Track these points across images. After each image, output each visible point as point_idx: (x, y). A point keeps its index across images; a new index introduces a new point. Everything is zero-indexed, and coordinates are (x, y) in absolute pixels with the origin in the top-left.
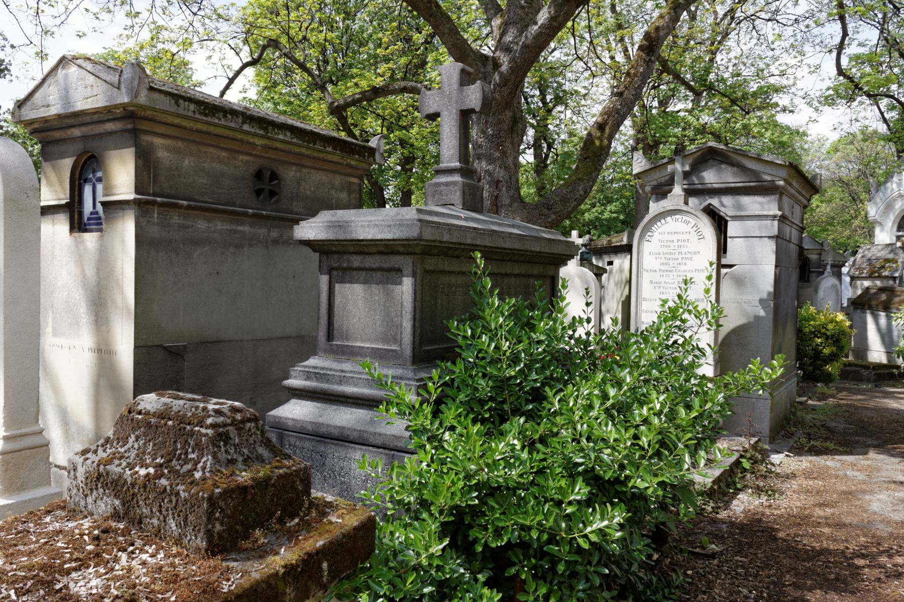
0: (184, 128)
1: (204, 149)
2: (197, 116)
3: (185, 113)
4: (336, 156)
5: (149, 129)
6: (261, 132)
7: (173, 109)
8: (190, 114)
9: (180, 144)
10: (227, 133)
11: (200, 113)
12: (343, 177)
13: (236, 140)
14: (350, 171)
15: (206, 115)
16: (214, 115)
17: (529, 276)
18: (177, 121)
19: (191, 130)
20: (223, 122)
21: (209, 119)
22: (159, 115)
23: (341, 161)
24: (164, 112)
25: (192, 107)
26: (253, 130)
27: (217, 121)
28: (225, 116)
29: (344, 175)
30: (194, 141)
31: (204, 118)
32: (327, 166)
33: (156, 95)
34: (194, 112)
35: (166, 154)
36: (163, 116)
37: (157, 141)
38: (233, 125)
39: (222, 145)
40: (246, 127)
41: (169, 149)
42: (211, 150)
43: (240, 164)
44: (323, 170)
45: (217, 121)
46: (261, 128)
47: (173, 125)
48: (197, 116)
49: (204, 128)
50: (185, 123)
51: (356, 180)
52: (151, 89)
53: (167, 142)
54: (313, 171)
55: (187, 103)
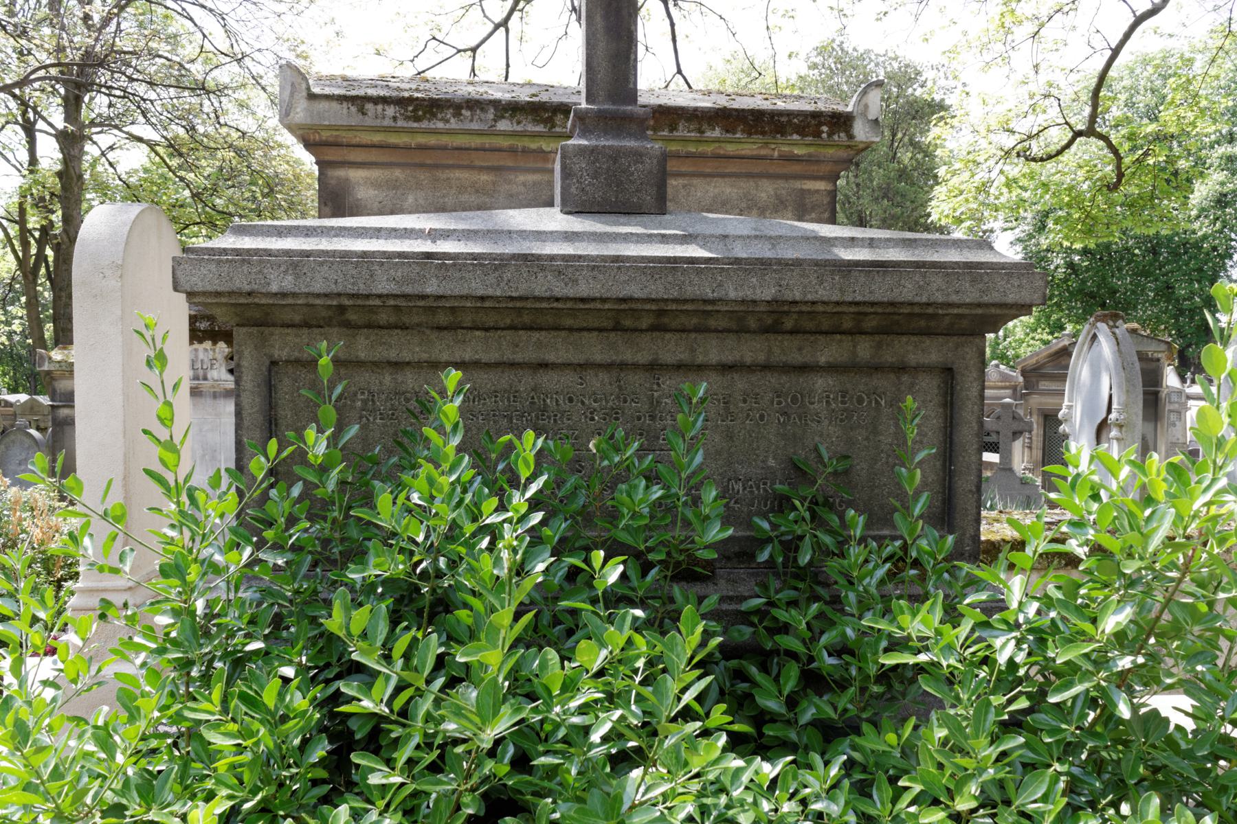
0: (395, 147)
1: (443, 175)
2: (401, 123)
3: (378, 122)
4: (749, 146)
5: (340, 159)
6: (540, 128)
7: (356, 119)
8: (387, 122)
9: (398, 173)
10: (476, 141)
11: (407, 118)
12: (781, 183)
13: (500, 150)
14: (796, 168)
15: (417, 119)
16: (434, 115)
17: (804, 369)
18: (377, 138)
19: (407, 148)
20: (454, 124)
21: (424, 124)
22: (344, 134)
23: (763, 152)
24: (350, 128)
25: (391, 111)
26: (519, 128)
27: (440, 125)
28: (457, 114)
29: (786, 177)
30: (422, 166)
31: (415, 125)
32: (732, 168)
33: (324, 105)
34: (395, 118)
35: (372, 192)
36: (350, 134)
37: (355, 175)
38: (475, 126)
39: (477, 163)
40: (504, 125)
41: (376, 185)
42: (458, 174)
43: (522, 189)
44: (723, 176)
45: (440, 125)
46: (536, 122)
47: (373, 146)
48: (401, 123)
49: (421, 139)
50: (393, 139)
51: (821, 186)
52: (312, 97)
53: (375, 174)
54: (695, 181)
55: (380, 107)
